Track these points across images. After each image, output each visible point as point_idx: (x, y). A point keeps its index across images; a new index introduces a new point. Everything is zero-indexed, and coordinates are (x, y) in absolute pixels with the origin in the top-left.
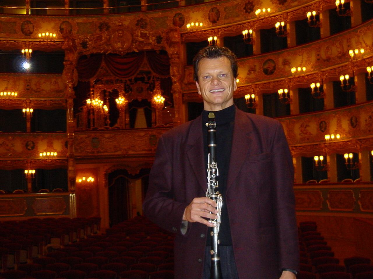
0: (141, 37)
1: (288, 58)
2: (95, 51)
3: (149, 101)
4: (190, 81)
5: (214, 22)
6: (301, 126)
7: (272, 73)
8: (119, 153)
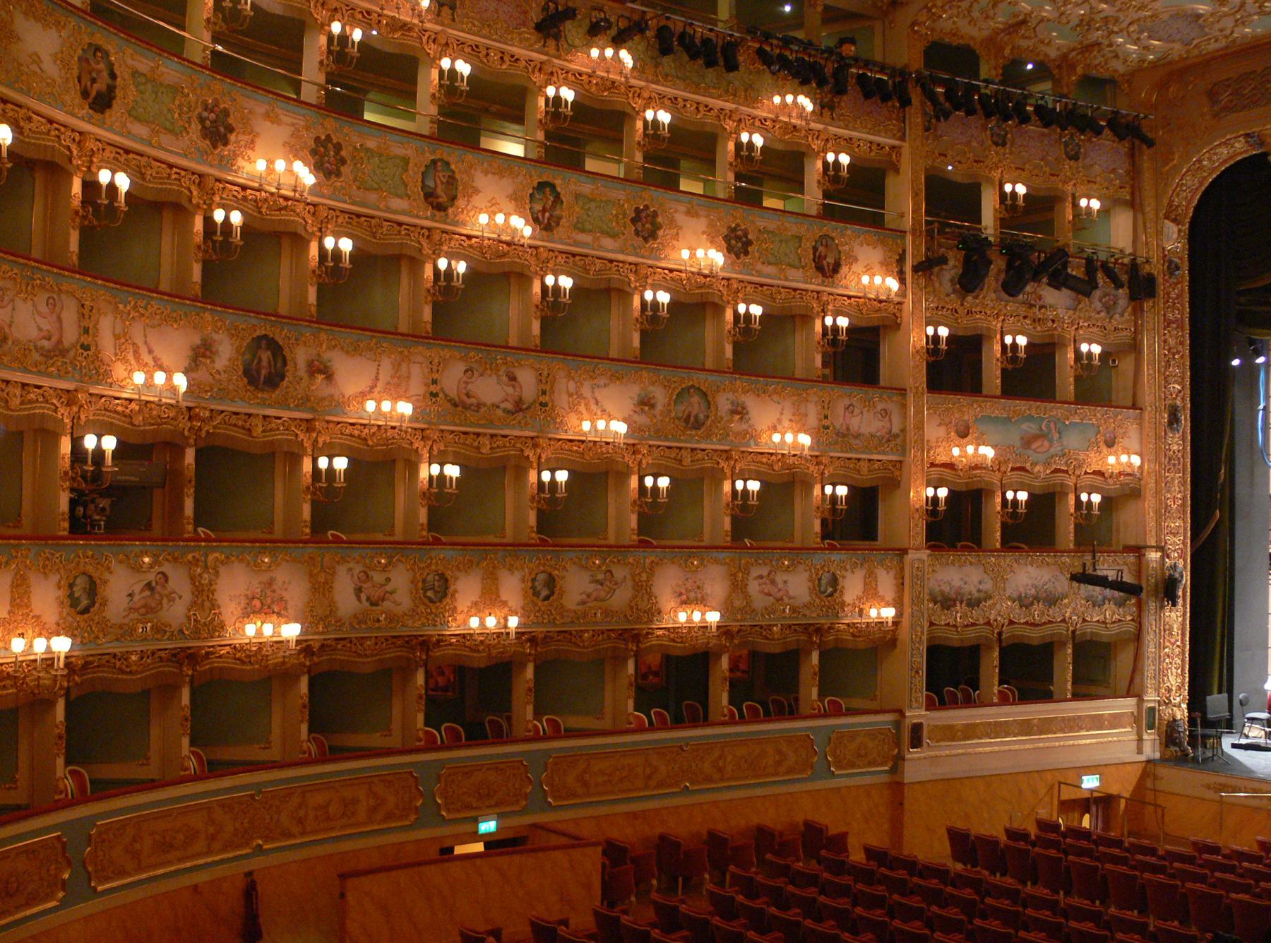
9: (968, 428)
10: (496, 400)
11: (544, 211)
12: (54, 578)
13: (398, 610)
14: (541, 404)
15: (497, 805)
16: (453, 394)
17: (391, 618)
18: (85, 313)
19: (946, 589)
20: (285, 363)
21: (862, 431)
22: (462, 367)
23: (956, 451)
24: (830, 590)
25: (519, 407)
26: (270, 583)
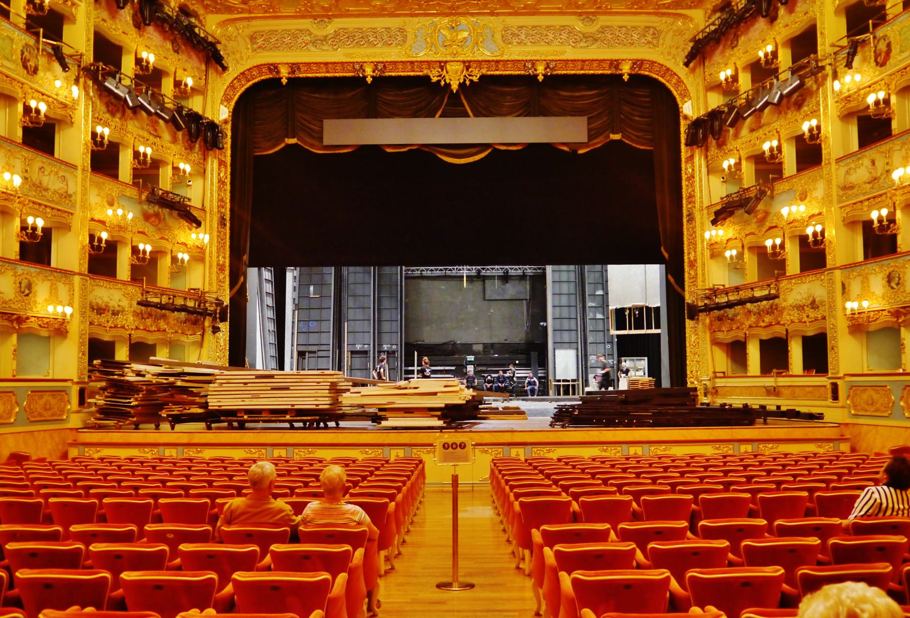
9: (113, 200)
19: (100, 302)
21: (49, 187)
23: (110, 212)
24: (27, 292)
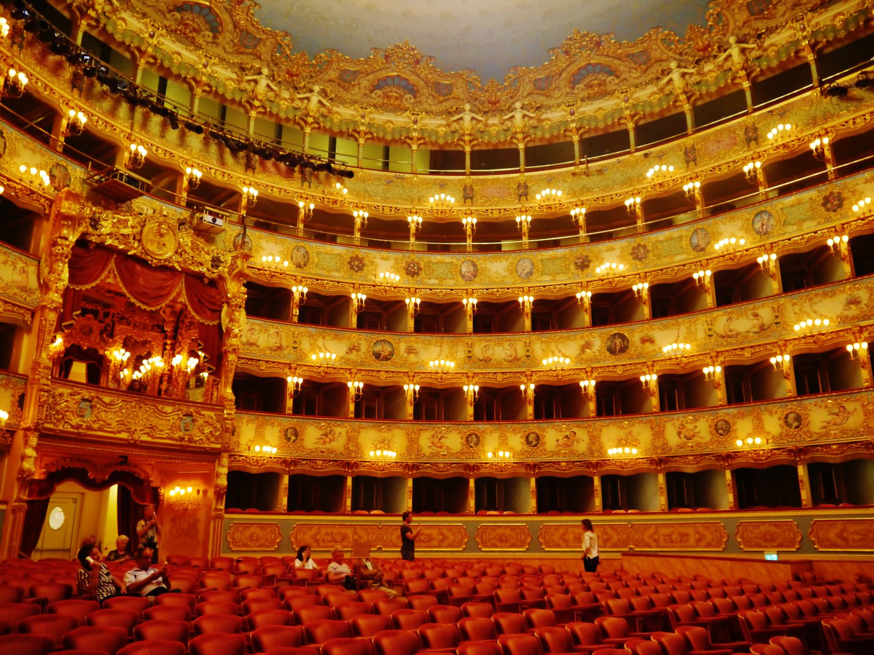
0: (192, 249)
1: (415, 346)
2: (109, 242)
3: (101, 352)
4: (251, 341)
5: (299, 266)
6: (433, 436)
7: (387, 359)
8: (124, 435)
10: (747, 329)
11: (763, 225)
12: (519, 435)
13: (704, 441)
14: (776, 323)
15: (778, 546)
16: (722, 332)
17: (698, 444)
18: (528, 345)
20: (628, 342)
22: (725, 318)
25: (762, 328)
26: (630, 433)
